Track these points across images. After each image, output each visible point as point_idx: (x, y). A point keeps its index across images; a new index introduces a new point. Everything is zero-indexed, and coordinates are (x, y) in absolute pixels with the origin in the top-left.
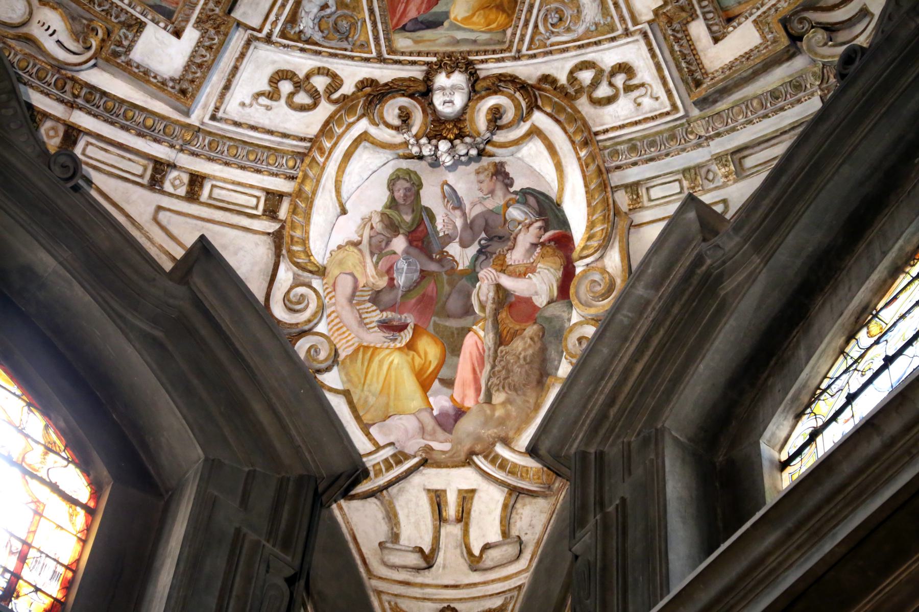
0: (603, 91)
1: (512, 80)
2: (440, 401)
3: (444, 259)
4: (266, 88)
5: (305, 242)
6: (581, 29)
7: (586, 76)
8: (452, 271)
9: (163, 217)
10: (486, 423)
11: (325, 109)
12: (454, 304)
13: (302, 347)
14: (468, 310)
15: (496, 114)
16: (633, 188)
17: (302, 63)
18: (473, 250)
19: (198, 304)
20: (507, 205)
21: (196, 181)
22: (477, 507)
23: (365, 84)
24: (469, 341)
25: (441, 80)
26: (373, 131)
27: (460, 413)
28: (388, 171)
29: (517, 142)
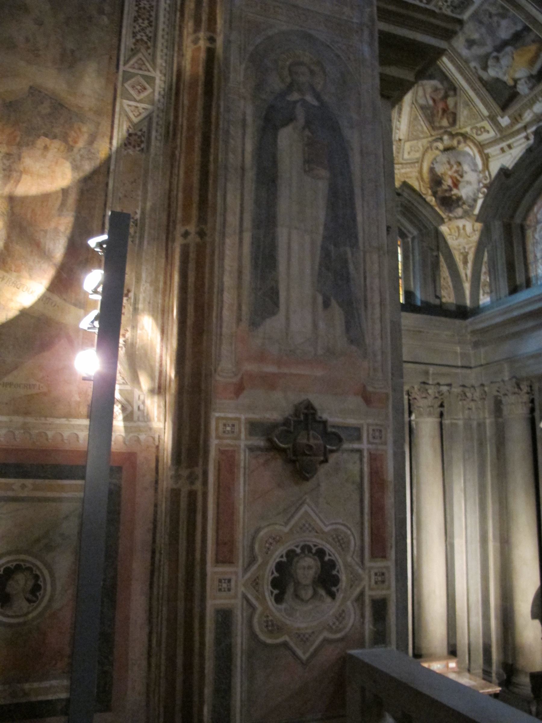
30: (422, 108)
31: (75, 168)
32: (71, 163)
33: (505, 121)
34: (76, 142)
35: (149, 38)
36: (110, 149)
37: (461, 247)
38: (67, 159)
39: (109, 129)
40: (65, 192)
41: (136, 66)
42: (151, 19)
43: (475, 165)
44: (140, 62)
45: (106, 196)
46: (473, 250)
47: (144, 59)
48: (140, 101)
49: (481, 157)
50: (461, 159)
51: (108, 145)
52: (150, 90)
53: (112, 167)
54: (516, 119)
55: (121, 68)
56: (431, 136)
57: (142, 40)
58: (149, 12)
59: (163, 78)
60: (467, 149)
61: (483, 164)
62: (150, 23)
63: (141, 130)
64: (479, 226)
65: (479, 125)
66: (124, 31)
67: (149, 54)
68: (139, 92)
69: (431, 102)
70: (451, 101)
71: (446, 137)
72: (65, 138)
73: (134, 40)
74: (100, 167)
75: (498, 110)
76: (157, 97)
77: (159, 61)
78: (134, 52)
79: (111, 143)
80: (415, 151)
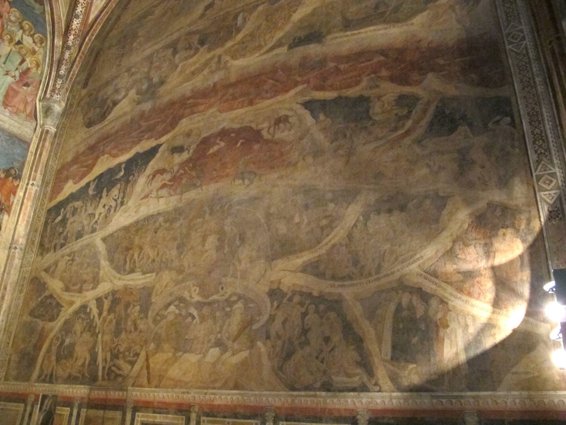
31: (523, 241)
32: (520, 239)
34: (520, 226)
35: (545, 150)
36: (541, 224)
38: (517, 237)
39: (537, 212)
40: (521, 257)
41: (542, 169)
42: (543, 138)
44: (544, 166)
45: (546, 253)
47: (546, 164)
48: (550, 190)
51: (539, 222)
52: (555, 181)
53: (545, 235)
55: (534, 175)
57: (541, 153)
58: (541, 134)
59: (561, 171)
62: (543, 141)
63: (556, 207)
66: (529, 153)
67: (548, 160)
68: (549, 185)
72: (513, 226)
73: (537, 155)
74: (538, 236)
76: (560, 182)
77: (555, 161)
78: (538, 162)
79: (540, 221)
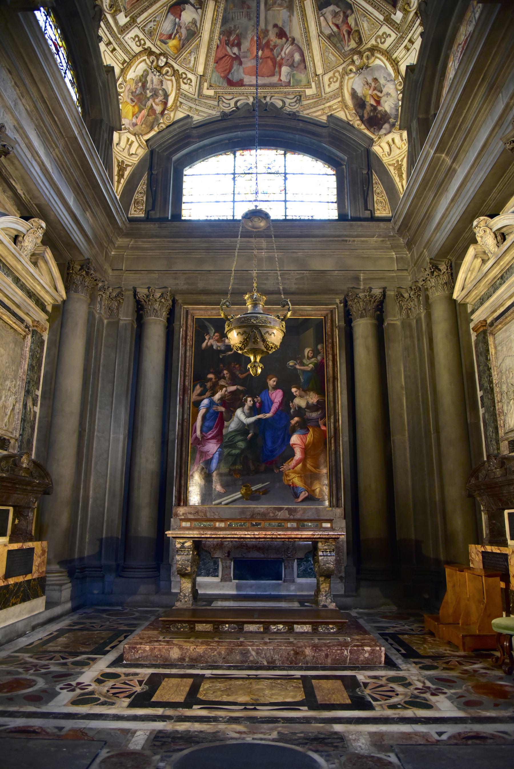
0: (185, 81)
1: (173, 67)
2: (134, 120)
3: (146, 93)
4: (134, 37)
5: (127, 75)
6: (188, 66)
7: (184, 76)
8: (146, 96)
9: (105, 52)
10: (140, 129)
11: (140, 49)
12: (144, 102)
13: (120, 97)
14: (145, 106)
15: (168, 72)
16: (181, 103)
17: (142, 36)
18: (151, 94)
19: (108, 81)
20: (160, 89)
21: (114, 49)
22: (133, 145)
23: (149, 47)
24: (143, 111)
25: (162, 58)
26: (147, 60)
27: (136, 125)
28: (144, 69)
29: (168, 80)
30: (329, 37)
33: (398, 16)
37: (394, 162)
43: (389, 75)
46: (405, 160)
49: (391, 64)
50: (376, 75)
54: (405, 10)
56: (344, 62)
60: (378, 62)
61: (394, 70)
64: (405, 134)
65: (380, 33)
69: (335, 29)
70: (351, 21)
71: (355, 57)
75: (390, 8)
80: (334, 82)
